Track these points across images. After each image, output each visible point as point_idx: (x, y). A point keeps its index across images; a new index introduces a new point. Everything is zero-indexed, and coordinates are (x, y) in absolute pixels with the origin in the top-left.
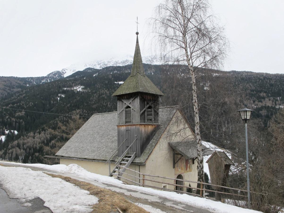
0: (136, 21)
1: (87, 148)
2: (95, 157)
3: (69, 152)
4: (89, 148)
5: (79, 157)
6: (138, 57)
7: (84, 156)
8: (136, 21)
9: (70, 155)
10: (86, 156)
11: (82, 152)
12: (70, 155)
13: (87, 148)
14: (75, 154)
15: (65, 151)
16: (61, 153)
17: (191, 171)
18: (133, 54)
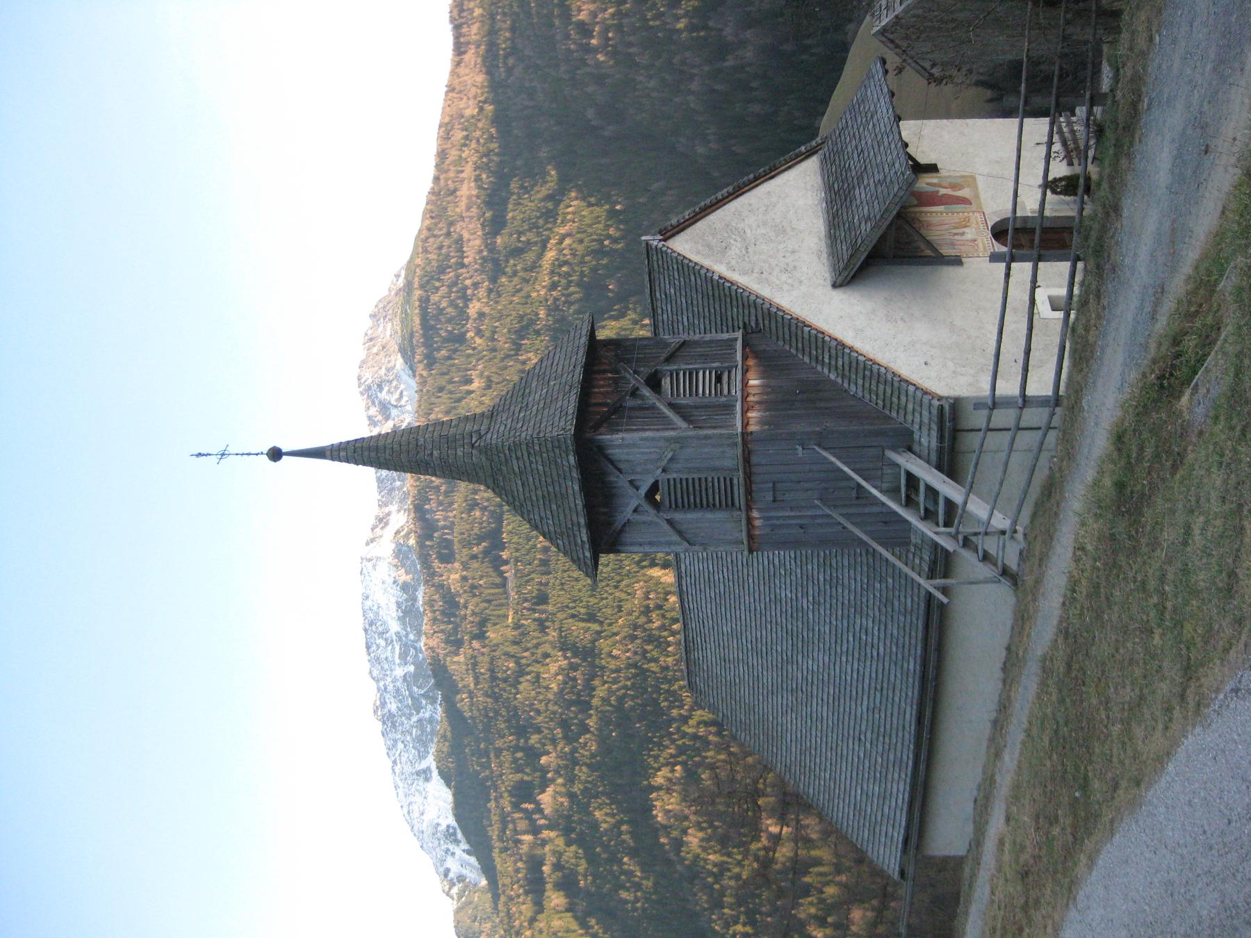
0: (214, 459)
1: (865, 717)
2: (911, 667)
3: (886, 810)
4: (865, 703)
5: (911, 756)
6: (421, 441)
7: (907, 725)
8: (214, 459)
9: (900, 802)
10: (908, 716)
11: (887, 740)
12: (900, 802)
13: (865, 717)
14: (896, 776)
15: (877, 831)
16: (874, 663)
17: (970, 180)
18: (367, 474)
